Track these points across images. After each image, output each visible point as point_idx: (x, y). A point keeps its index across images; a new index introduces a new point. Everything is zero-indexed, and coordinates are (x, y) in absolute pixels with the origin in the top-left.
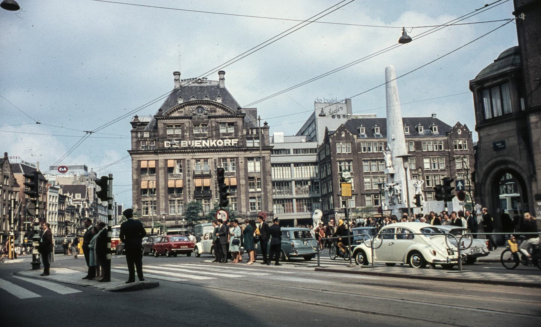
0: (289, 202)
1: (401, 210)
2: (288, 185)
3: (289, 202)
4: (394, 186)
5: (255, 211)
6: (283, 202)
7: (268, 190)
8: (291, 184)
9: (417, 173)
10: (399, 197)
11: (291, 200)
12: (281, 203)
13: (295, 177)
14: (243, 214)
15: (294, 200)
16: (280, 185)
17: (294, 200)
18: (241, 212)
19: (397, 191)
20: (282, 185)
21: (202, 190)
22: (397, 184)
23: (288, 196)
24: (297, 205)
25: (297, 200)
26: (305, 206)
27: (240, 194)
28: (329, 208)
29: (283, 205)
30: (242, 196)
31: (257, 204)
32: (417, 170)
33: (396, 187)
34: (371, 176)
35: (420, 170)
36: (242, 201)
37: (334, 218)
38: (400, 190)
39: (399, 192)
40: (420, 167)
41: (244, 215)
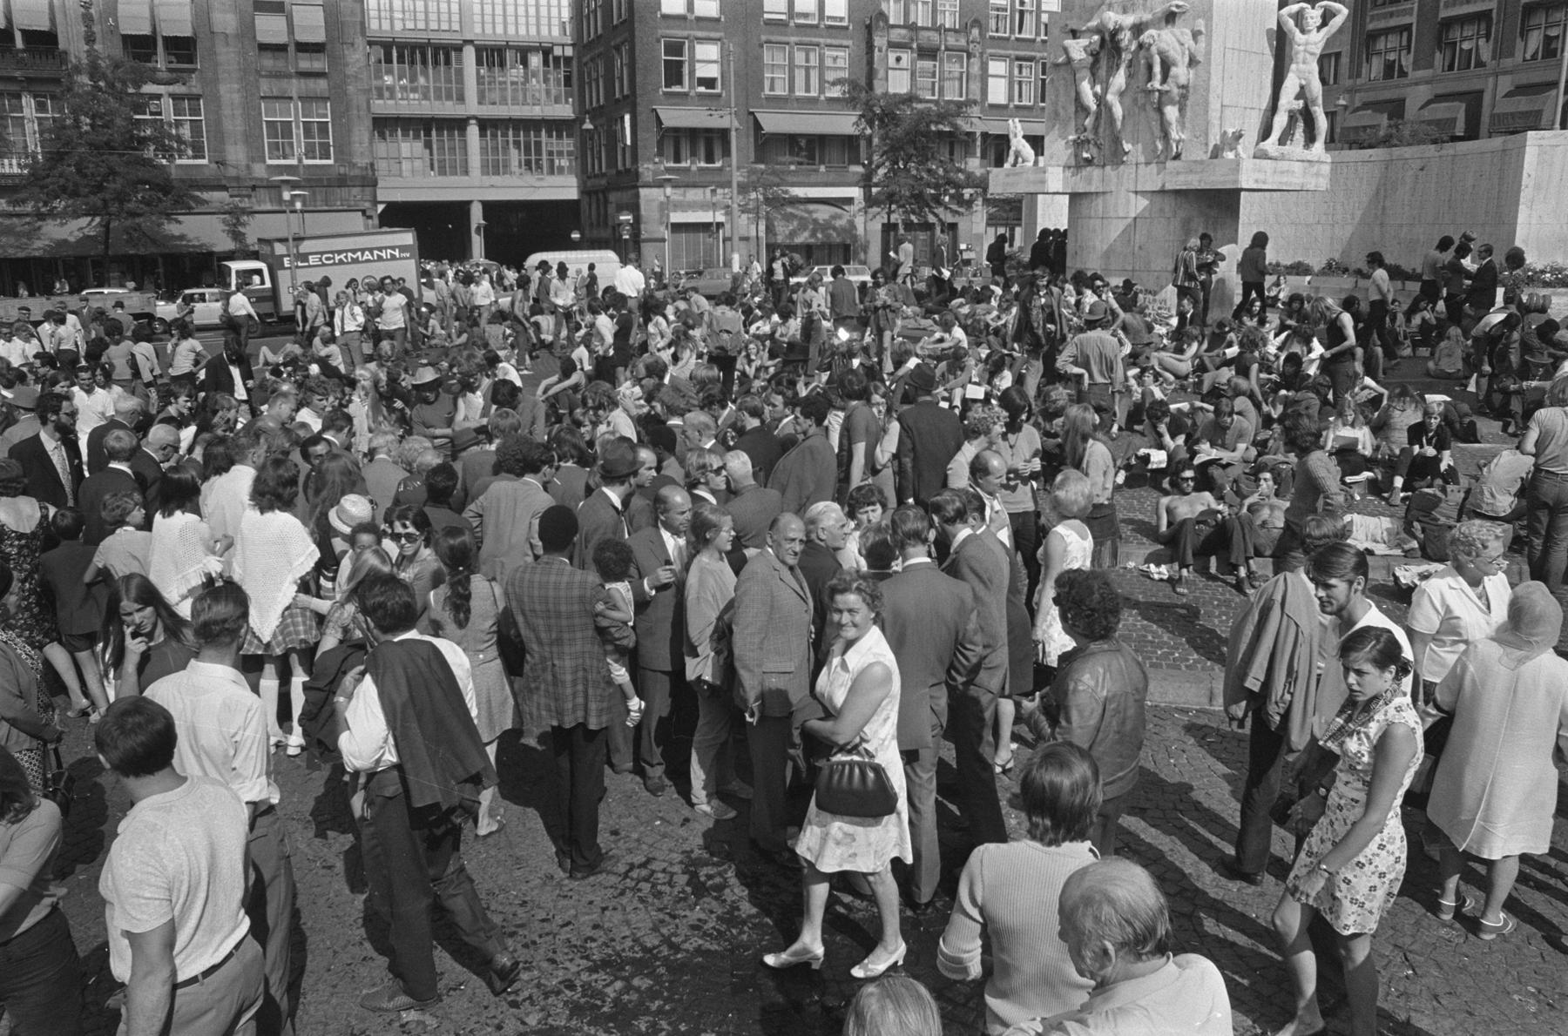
0: (451, 135)
1: (1168, 204)
2: (448, 62)
3: (451, 135)
4: (1138, 29)
5: (294, 162)
6: (428, 134)
7: (350, 71)
8: (460, 61)
9: (963, 42)
10: (1171, 112)
11: (460, 124)
12: (417, 137)
13: (478, 30)
14: (232, 172)
15: (473, 131)
16: (412, 62)
17: (473, 131)
18: (221, 163)
19: (1166, 66)
20: (424, 62)
21: (19, 43)
22: (1170, 17)
23: (448, 109)
24: (484, 150)
25: (485, 125)
26: (514, 152)
27: (216, 81)
28: (612, 161)
29: (428, 145)
30: (223, 89)
31: (298, 133)
32: (964, 30)
33: (1166, 39)
34: (793, 39)
35: (975, 32)
36: (226, 111)
37: (634, 208)
38: (1193, 62)
39: (1181, 72)
40: (977, 23)
41: (237, 179)
